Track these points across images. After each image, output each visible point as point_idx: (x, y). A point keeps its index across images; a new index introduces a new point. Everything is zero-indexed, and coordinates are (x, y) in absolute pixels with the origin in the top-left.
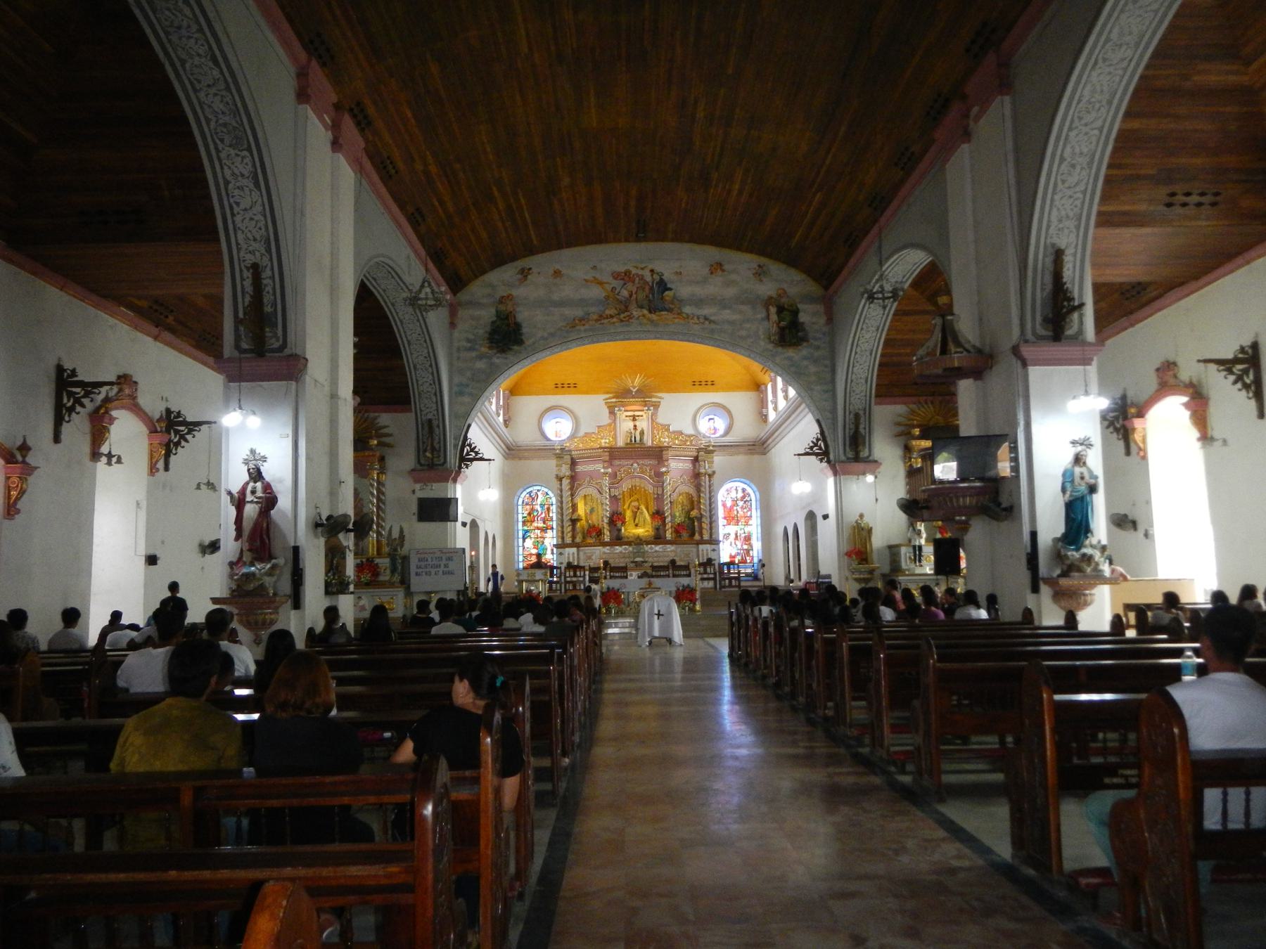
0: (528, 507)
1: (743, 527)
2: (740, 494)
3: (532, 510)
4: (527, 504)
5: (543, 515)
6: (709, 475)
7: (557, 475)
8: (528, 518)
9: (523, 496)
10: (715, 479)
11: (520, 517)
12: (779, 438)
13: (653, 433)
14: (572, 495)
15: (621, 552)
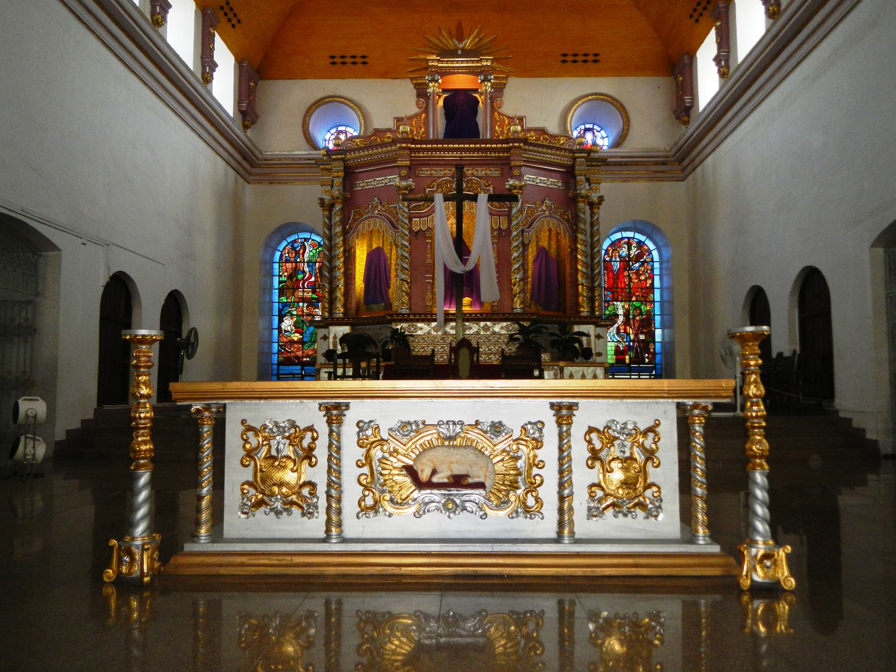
0: (289, 265)
1: (637, 304)
2: (634, 251)
3: (296, 271)
4: (287, 261)
5: (313, 279)
6: (592, 205)
7: (322, 201)
8: (289, 283)
9: (281, 248)
10: (603, 213)
11: (276, 280)
12: (699, 158)
13: (493, 130)
14: (345, 233)
15: (429, 333)
